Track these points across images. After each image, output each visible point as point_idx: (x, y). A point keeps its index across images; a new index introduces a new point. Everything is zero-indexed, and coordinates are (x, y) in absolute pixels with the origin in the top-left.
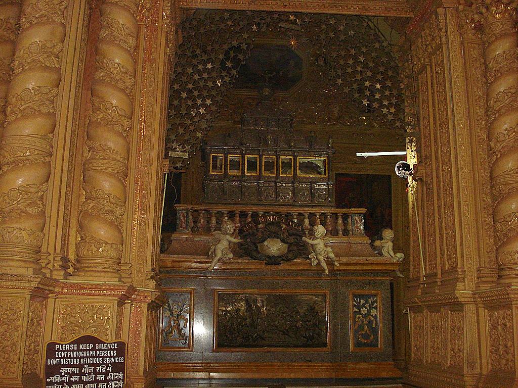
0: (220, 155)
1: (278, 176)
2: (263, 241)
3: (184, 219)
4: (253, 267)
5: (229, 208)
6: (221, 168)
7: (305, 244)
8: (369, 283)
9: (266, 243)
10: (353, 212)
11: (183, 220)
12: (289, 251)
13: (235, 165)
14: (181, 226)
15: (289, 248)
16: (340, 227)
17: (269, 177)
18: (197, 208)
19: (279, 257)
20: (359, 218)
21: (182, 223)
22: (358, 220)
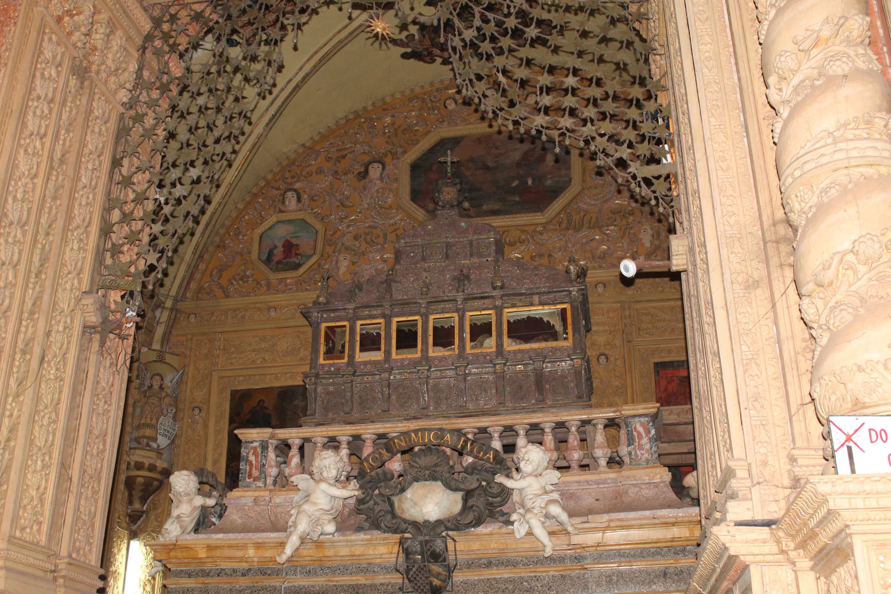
1: (462, 354)
2: (403, 490)
3: (256, 461)
4: (382, 550)
5: (351, 430)
6: (343, 352)
7: (505, 493)
8: (665, 574)
9: (409, 493)
11: (254, 462)
12: (465, 508)
13: (370, 342)
14: (250, 476)
15: (465, 500)
16: (601, 454)
17: (442, 359)
18: (283, 433)
19: (439, 522)
20: (642, 424)
21: (251, 469)
22: (640, 429)
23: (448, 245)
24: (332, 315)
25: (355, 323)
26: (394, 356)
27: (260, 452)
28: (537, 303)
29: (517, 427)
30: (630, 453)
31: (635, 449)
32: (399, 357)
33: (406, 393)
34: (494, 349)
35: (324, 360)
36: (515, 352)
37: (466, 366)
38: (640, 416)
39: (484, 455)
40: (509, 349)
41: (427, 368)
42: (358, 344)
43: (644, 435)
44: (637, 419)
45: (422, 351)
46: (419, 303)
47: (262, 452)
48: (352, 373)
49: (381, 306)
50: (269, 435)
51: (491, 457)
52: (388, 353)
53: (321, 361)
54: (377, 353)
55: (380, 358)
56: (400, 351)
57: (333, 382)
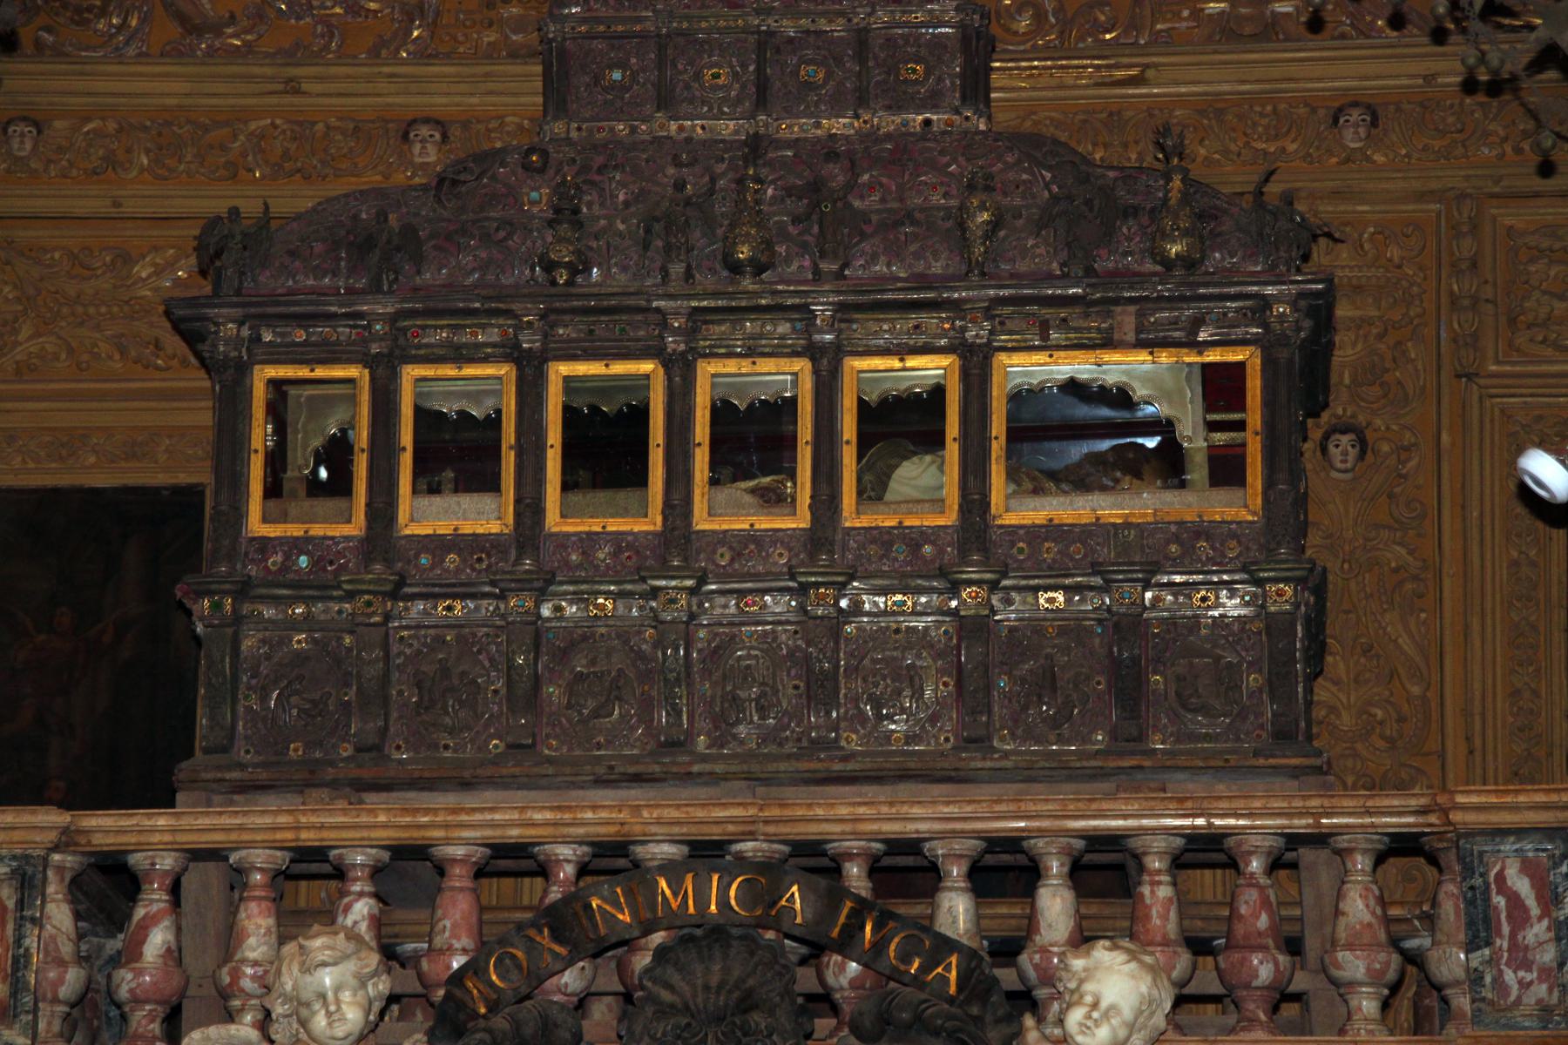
0: (338, 372)
10: (1471, 817)
20: (1528, 868)
22: (1523, 886)
23: (767, 43)
24: (300, 336)
25: (394, 376)
26: (554, 520)
27: (11, 904)
28: (1131, 337)
29: (1041, 843)
30: (1475, 978)
31: (1492, 962)
32: (572, 527)
33: (599, 676)
34: (949, 518)
35: (265, 519)
36: (1036, 534)
37: (844, 585)
38: (1520, 832)
39: (925, 968)
40: (1010, 519)
41: (689, 583)
42: (406, 461)
43: (1535, 911)
44: (1508, 846)
45: (668, 506)
46: (658, 310)
47: (21, 905)
48: (388, 588)
49: (508, 313)
50: (52, 836)
51: (953, 975)
52: (530, 508)
53: (256, 525)
54: (486, 501)
55: (495, 527)
56: (576, 498)
57: (307, 616)
